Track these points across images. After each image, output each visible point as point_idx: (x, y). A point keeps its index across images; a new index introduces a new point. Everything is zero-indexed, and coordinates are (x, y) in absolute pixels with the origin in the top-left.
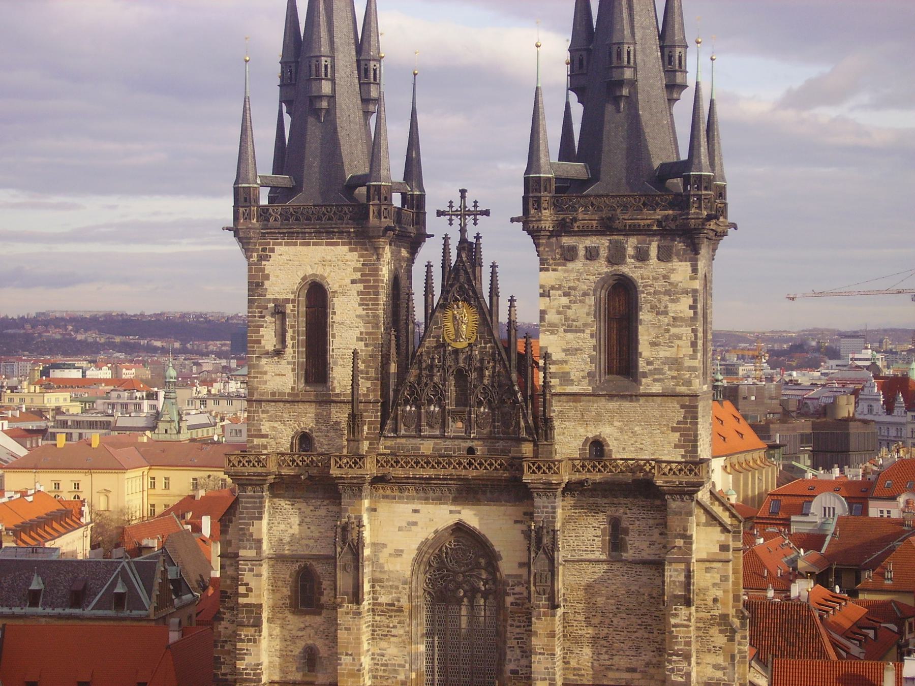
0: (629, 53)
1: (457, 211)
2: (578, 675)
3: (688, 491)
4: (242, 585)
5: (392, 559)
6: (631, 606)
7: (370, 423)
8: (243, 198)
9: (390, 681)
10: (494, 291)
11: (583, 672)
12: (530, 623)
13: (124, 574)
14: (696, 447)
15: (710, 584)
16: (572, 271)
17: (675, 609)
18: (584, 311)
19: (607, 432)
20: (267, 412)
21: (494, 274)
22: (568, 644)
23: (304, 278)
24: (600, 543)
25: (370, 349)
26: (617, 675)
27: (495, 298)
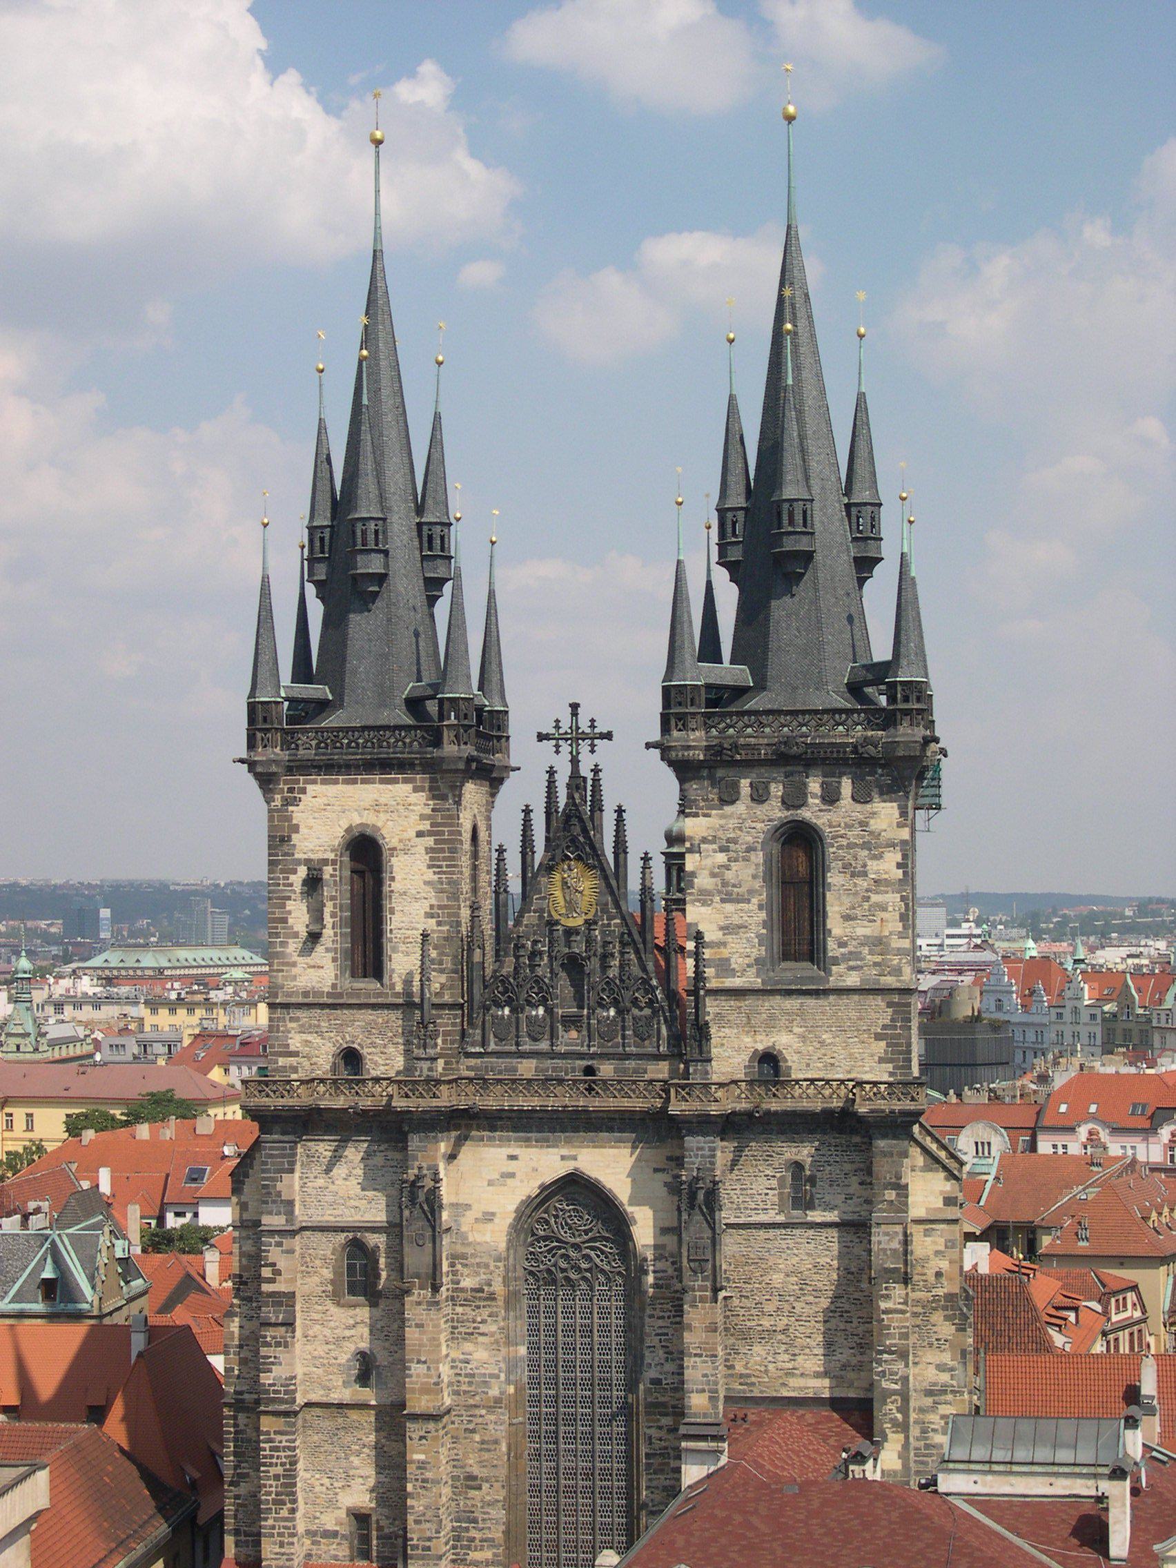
0: (805, 512)
1: (566, 733)
2: (746, 1384)
4: (266, 1265)
5: (480, 1226)
6: (820, 1285)
7: (446, 1034)
8: (259, 719)
9: (477, 1398)
10: (620, 846)
11: (753, 1379)
12: (679, 1311)
15: (930, 1253)
16: (731, 816)
17: (886, 1288)
18: (749, 873)
19: (784, 1041)
20: (297, 1019)
21: (620, 821)
22: (732, 1340)
24: (776, 1199)
25: (446, 928)
26: (800, 1382)
27: (622, 856)
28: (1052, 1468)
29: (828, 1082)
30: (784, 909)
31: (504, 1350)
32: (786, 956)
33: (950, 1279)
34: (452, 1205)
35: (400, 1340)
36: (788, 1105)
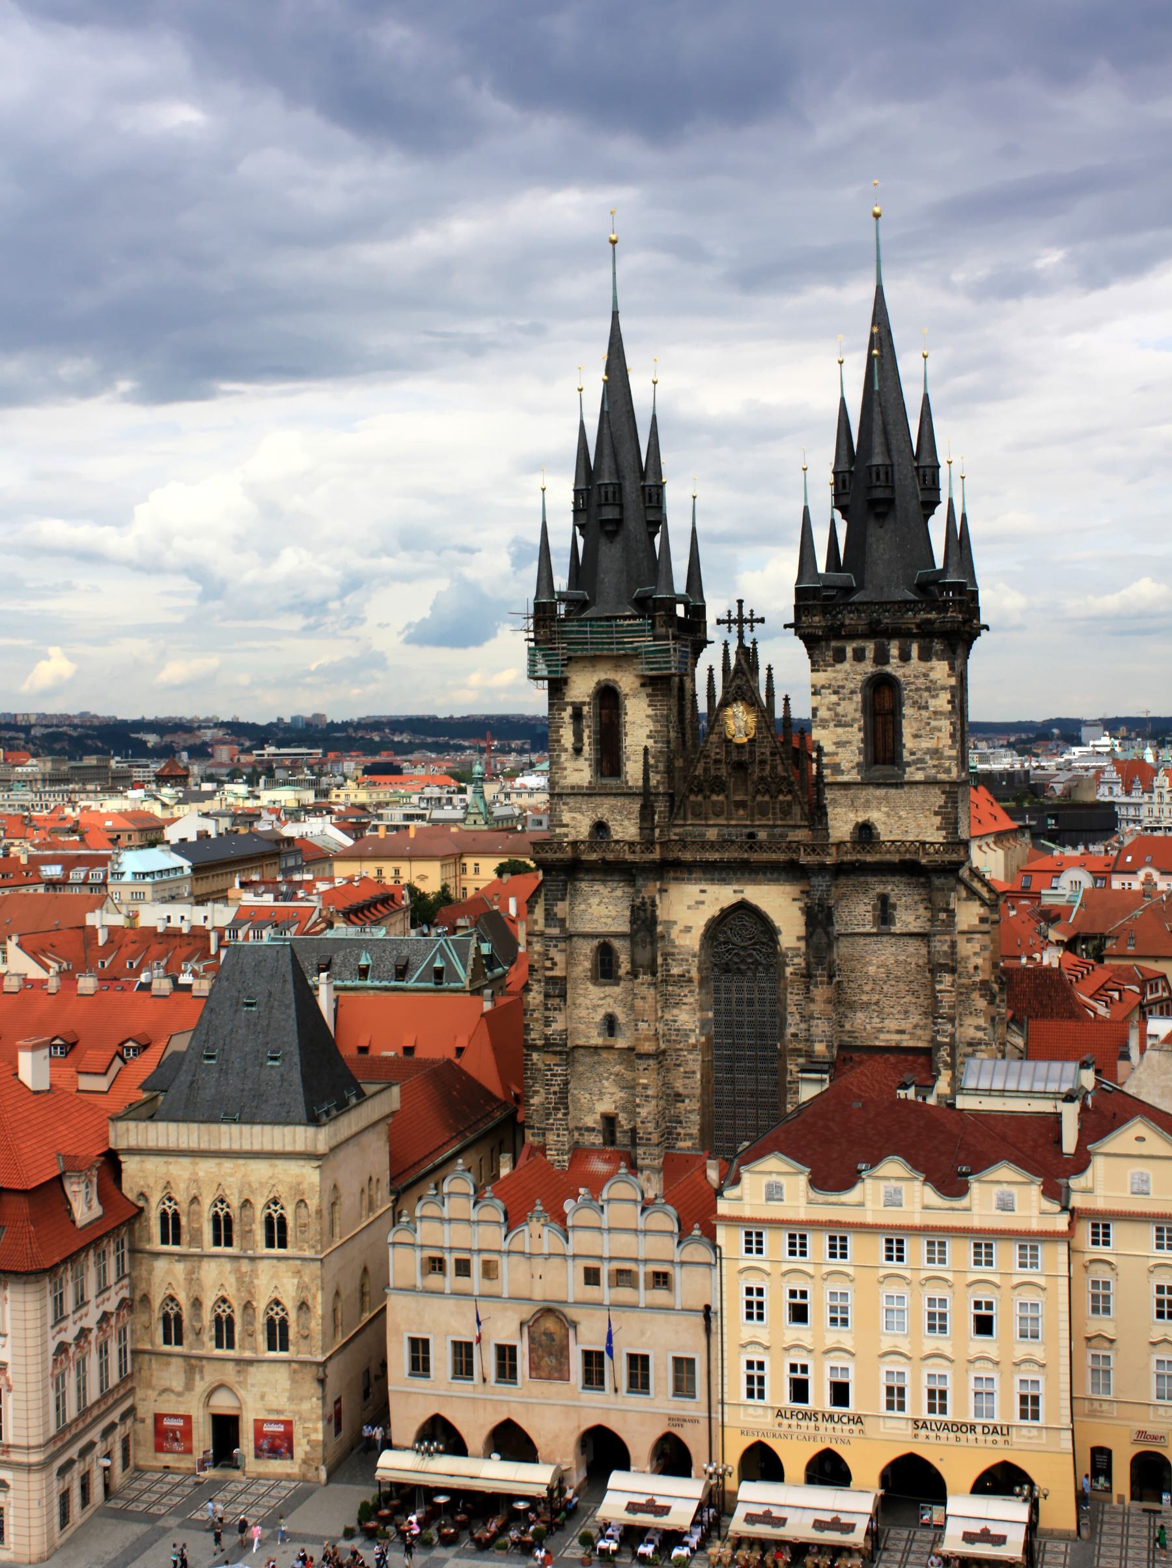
3: (951, 870)
7: (660, 812)
8: (543, 614)
12: (808, 989)
13: (441, 950)
14: (957, 829)
15: (970, 953)
18: (852, 708)
19: (876, 816)
21: (770, 677)
23: (598, 683)
24: (871, 918)
28: (1031, 1094)
29: (903, 842)
30: (875, 732)
31: (698, 1015)
32: (876, 762)
33: (984, 971)
34: (666, 922)
35: (632, 1008)
36: (877, 858)
